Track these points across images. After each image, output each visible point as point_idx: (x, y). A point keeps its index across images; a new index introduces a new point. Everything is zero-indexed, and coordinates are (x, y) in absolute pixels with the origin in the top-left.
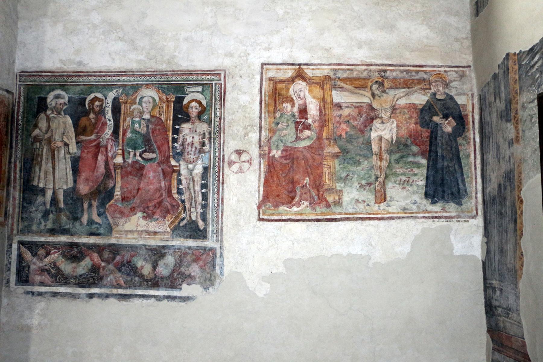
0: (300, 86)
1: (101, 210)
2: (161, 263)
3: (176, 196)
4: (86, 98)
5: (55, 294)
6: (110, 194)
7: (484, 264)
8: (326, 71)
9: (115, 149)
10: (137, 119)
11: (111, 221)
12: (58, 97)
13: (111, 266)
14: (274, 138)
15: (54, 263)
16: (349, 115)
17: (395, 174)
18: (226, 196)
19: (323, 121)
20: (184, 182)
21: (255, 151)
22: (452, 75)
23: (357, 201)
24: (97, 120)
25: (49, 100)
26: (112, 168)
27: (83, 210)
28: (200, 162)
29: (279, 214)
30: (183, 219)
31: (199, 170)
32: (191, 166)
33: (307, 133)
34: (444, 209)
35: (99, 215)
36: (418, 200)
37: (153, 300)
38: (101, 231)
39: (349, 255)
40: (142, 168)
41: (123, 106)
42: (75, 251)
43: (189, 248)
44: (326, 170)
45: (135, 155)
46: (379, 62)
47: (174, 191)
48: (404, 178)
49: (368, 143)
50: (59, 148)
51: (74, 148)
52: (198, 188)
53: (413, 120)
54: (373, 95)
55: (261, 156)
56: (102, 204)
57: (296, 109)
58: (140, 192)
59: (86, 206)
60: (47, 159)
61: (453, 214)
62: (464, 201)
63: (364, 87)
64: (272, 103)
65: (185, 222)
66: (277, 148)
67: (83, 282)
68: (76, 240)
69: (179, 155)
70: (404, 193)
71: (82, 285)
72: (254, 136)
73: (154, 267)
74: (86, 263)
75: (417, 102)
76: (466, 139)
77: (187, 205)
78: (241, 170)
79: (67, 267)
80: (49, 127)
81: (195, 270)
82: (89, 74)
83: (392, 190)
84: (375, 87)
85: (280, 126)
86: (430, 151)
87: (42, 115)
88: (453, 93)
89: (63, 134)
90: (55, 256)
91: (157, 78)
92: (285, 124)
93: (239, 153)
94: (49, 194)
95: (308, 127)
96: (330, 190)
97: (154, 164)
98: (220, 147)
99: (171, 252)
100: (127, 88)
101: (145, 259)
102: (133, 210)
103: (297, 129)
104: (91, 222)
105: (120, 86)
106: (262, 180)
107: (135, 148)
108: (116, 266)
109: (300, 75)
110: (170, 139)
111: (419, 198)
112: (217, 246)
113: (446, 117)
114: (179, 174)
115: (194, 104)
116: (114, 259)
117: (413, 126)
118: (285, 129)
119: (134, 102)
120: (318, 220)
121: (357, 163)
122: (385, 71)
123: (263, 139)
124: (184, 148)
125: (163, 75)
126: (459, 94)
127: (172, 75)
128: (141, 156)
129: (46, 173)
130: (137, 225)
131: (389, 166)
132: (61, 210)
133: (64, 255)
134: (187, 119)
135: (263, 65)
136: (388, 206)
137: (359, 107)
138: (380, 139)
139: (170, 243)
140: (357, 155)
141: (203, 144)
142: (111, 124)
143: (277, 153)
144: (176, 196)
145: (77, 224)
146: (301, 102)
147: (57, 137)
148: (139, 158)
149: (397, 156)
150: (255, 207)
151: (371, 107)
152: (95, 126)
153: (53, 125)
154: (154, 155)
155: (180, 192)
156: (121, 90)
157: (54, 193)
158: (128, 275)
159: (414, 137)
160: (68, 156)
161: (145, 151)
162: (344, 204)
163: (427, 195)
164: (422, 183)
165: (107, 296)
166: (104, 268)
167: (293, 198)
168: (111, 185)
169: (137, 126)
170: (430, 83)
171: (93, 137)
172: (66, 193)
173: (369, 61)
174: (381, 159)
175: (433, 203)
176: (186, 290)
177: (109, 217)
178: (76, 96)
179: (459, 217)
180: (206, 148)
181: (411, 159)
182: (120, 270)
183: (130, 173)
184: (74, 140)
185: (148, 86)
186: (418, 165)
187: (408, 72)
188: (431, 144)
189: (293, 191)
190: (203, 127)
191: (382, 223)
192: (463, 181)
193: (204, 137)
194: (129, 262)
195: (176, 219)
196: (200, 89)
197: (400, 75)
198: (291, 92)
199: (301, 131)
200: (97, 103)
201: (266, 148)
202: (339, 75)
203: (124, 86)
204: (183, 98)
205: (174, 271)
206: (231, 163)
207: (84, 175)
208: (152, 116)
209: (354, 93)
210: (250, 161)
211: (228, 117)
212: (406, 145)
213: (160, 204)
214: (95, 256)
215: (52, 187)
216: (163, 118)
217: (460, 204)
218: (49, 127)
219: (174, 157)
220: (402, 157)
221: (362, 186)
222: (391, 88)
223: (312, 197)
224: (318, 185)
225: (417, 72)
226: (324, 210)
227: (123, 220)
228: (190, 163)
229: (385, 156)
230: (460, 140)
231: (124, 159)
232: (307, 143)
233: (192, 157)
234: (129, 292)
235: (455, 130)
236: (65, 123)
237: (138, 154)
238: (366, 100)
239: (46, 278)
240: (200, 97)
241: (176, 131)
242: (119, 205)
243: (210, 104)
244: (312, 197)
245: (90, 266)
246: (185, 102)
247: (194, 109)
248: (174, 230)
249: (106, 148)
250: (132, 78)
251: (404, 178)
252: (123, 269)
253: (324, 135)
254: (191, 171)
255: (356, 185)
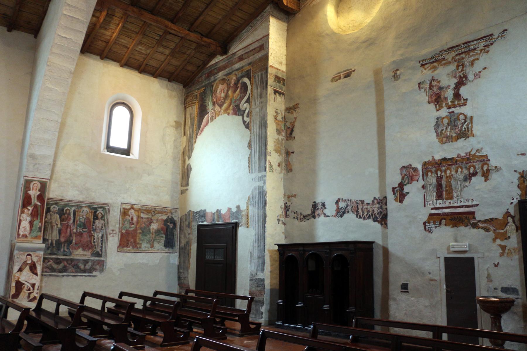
0: (132, 211)
1: (68, 247)
2: (87, 265)
3: (93, 243)
4: (64, 209)
5: (50, 275)
6: (71, 242)
7: (178, 266)
8: (139, 207)
9: (73, 227)
10: (81, 217)
11: (71, 251)
12: (54, 208)
13: (70, 266)
14: (123, 227)
15: (51, 265)
16: (145, 221)
17: (156, 239)
18: (108, 243)
19: (138, 222)
20: (96, 239)
21: (117, 231)
22: (173, 211)
23: (146, 247)
24: (68, 217)
25: (51, 209)
26: (72, 233)
27: (61, 247)
28: (101, 233)
29: (124, 250)
30: (95, 251)
31: (100, 235)
32: (98, 234)
33: (133, 226)
34: (169, 250)
35: (67, 249)
36: (162, 247)
37: (84, 277)
38: (68, 254)
39: (143, 263)
40: (82, 234)
41: (77, 213)
42: (58, 261)
43: (96, 260)
44: (138, 238)
45: (80, 229)
46: (154, 205)
47: (92, 242)
48: (159, 241)
49: (150, 230)
50: (54, 225)
51: (59, 226)
52: (100, 241)
53: (162, 224)
54: (152, 215)
55: (119, 232)
56: (69, 245)
57: (130, 218)
58: (81, 242)
59: (63, 245)
60: (50, 229)
61: (171, 252)
62: (174, 248)
63: (150, 213)
64: (123, 215)
65: (95, 252)
66: (124, 230)
67: (61, 271)
68: (59, 257)
69: (94, 230)
70: (158, 245)
71: (60, 272)
72: (117, 226)
73: (85, 266)
74: (62, 265)
75: (164, 218)
76: (176, 230)
77: (96, 246)
78: (113, 236)
79: (55, 266)
80: (51, 218)
81: (98, 267)
82: (65, 201)
83: (156, 244)
84: (153, 213)
85: (125, 223)
86: (166, 233)
87: (49, 214)
88: (173, 216)
89: (56, 221)
90: (51, 262)
91: (89, 204)
92: (127, 223)
93: (113, 230)
94: (50, 241)
95: (133, 224)
96: (139, 243)
97: (86, 233)
98: (107, 229)
99: (90, 261)
100: (79, 207)
101: (82, 264)
102: (79, 248)
103: (130, 224)
104: (64, 251)
105: (76, 206)
106: (119, 240)
107: (80, 227)
108: (72, 266)
109: (132, 208)
110: (92, 225)
111: (162, 247)
112: (105, 259)
113: (171, 223)
114: (94, 236)
115: (100, 214)
116: (71, 263)
117: (162, 225)
118: (127, 224)
119: (80, 212)
120: (134, 252)
121: (146, 236)
122: (156, 208)
123: (120, 227)
124: (96, 228)
125: (90, 204)
126: (175, 217)
127: (94, 204)
128: (82, 230)
129: (49, 234)
130: (80, 252)
131: (155, 237)
132: (53, 247)
133: (54, 262)
134: (97, 219)
135: (122, 203)
136: (154, 249)
137: (148, 219)
138: (153, 229)
139: (90, 259)
140: (146, 233)
141: (102, 227)
142: (72, 218)
143: (124, 231)
144: (93, 243)
145: (59, 252)
146: (132, 216)
147: (54, 221)
148: (81, 231)
149: (157, 234)
150: (117, 248)
151: (151, 219)
152: (67, 219)
153: (52, 218)
154: (86, 230)
155: (94, 242)
156: (76, 207)
157: (52, 241)
158: (76, 268)
159: (162, 229)
160: (57, 228)
161: (83, 228)
162: (142, 247)
163: (164, 246)
164: (163, 242)
165: (69, 276)
166: (68, 266)
167: (128, 245)
168: (72, 239)
169: (81, 219)
170: (167, 213)
171: (66, 222)
172: (56, 241)
173: (152, 205)
174: (153, 235)
175: (166, 248)
176: (95, 273)
177: (70, 249)
178: (61, 208)
179: (172, 252)
180: (103, 229)
181: (161, 235)
182: (73, 267)
183: (78, 235)
184: (60, 223)
185: (85, 207)
186: (163, 237)
187: (162, 209)
188: (166, 231)
189: (128, 243)
190: (102, 222)
191: (152, 254)
192: (174, 242)
193: (102, 225)
194: (77, 265)
195: (92, 251)
196: (102, 209)
197: (160, 210)
198: (129, 213)
199: (131, 225)
200: (68, 211)
201: (121, 230)
202: (143, 208)
203: (77, 206)
204: (96, 212)
205: (91, 267)
206: (110, 234)
207: (62, 235)
208: (87, 217)
209: (147, 214)
210: (116, 233)
211: (110, 219)
212: (160, 231)
213: (88, 246)
214: (65, 262)
215: (51, 238)
216: (90, 218)
217: (173, 249)
218: (51, 218)
219: (93, 231)
220: (158, 234)
221: (147, 242)
222: (157, 214)
223: (133, 245)
224: (135, 242)
225: (164, 209)
226: (136, 249)
227: (75, 251)
228: (98, 233)
229: (154, 234)
230: (174, 230)
231: (76, 230)
232: (133, 229)
233: (98, 231)
234: (76, 274)
235: (173, 227)
236: (56, 217)
237: (81, 229)
238: (150, 217)
239: (48, 270)
240: (102, 212)
241: (94, 223)
242: (74, 245)
243: (105, 215)
244: (133, 245)
245: (63, 266)
246: (97, 213)
247: (100, 216)
248: (92, 254)
249: (70, 226)
250: (80, 204)
251: (159, 241)
252: (75, 267)
253: (138, 227)
254: (98, 236)
255: (146, 242)
